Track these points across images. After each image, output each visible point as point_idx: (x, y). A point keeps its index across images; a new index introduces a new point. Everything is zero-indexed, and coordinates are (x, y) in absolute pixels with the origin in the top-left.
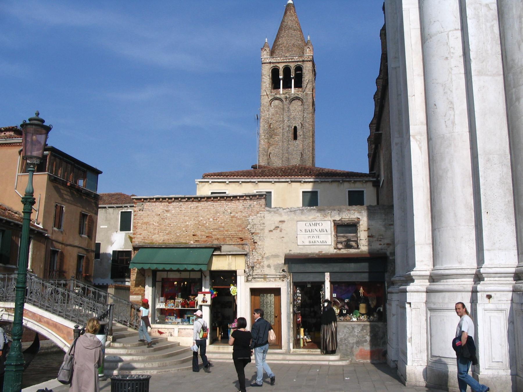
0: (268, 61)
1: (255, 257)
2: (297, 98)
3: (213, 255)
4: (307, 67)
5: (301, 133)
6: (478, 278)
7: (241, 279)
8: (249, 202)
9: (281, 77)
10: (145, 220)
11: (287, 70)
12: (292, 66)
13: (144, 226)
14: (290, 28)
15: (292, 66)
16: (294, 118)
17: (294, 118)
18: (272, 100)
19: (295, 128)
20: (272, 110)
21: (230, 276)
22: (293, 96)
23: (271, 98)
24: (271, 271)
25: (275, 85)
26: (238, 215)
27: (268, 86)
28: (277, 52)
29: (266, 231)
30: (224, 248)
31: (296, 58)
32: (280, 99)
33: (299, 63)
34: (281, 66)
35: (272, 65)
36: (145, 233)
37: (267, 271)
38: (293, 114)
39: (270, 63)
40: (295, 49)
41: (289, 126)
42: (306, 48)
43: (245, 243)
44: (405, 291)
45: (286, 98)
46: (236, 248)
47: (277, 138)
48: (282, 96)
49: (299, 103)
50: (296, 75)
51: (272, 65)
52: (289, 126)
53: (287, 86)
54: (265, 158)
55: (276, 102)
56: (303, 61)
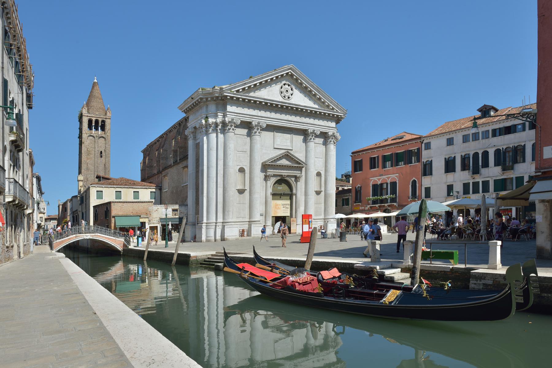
2: (103, 137)
4: (108, 122)
6: (216, 223)
9: (93, 124)
11: (97, 121)
12: (100, 120)
14: (97, 98)
15: (100, 120)
16: (101, 147)
17: (101, 147)
18: (89, 136)
19: (101, 152)
20: (88, 141)
21: (143, 224)
22: (100, 136)
25: (90, 127)
28: (90, 111)
32: (93, 136)
34: (94, 119)
38: (100, 145)
43: (148, 214)
47: (91, 156)
48: (95, 135)
49: (104, 139)
53: (97, 129)
54: (85, 165)
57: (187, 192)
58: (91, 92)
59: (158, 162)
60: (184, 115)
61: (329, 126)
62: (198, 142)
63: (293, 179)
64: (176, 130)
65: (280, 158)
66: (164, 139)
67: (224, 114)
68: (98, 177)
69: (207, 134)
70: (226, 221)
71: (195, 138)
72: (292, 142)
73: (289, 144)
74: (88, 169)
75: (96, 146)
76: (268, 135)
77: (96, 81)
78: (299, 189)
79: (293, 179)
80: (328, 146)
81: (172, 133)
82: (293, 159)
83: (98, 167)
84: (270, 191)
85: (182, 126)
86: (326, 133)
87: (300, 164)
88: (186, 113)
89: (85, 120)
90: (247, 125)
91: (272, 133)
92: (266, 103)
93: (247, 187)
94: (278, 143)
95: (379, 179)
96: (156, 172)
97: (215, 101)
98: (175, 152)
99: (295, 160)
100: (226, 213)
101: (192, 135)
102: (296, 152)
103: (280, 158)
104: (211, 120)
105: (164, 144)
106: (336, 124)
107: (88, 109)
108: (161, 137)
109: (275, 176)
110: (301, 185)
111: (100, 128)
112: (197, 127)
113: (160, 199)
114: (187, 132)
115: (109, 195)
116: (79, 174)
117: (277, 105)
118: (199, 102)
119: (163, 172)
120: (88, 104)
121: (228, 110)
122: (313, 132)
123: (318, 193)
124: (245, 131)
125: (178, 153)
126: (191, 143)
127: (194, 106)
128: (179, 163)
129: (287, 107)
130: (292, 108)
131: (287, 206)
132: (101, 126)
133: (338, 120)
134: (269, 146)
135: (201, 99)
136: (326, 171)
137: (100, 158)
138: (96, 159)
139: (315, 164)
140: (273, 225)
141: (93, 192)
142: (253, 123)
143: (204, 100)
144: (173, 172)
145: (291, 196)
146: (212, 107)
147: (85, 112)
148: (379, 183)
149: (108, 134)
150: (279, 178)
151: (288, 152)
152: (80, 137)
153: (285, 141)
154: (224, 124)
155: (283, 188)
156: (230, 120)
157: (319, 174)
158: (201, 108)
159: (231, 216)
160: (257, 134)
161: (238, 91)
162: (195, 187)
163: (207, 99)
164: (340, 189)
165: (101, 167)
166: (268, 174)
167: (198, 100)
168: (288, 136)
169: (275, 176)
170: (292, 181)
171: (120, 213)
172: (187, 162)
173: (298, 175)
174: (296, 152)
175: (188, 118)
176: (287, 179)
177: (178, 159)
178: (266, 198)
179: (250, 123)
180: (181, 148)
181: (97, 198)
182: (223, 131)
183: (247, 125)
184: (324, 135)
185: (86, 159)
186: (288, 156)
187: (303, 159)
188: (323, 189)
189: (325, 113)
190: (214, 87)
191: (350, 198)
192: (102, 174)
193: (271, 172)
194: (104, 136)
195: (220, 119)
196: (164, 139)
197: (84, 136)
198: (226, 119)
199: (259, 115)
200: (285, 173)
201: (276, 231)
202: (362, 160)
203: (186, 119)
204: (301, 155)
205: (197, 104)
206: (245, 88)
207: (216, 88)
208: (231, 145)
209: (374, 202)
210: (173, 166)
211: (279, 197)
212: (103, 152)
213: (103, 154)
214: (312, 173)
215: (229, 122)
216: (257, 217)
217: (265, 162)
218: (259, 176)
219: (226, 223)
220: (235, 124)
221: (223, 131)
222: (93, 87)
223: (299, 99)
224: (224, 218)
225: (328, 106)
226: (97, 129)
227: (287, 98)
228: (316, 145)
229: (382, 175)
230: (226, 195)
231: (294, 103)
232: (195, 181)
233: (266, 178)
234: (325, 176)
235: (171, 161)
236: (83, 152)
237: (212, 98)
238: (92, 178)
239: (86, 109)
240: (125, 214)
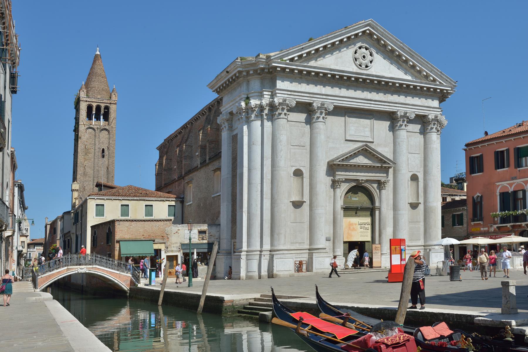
0: (84, 99)
4: (113, 108)
5: (107, 154)
6: (261, 251)
9: (94, 112)
11: (98, 108)
12: (103, 105)
15: (103, 105)
16: (103, 143)
17: (103, 143)
18: (88, 128)
19: (103, 150)
20: (87, 136)
22: (103, 127)
23: (87, 127)
25: (89, 116)
26: (161, 227)
27: (84, 118)
28: (90, 94)
31: (105, 101)
33: (107, 105)
34: (94, 105)
35: (88, 103)
38: (102, 140)
39: (86, 101)
40: (104, 92)
41: (99, 148)
42: (112, 94)
44: (240, 255)
45: (98, 128)
47: (90, 156)
48: (95, 127)
49: (107, 133)
50: (104, 111)
51: (88, 103)
52: (99, 148)
53: (98, 118)
54: (82, 169)
55: (90, 130)
56: (110, 103)
57: (219, 206)
58: (92, 68)
59: (180, 162)
60: (215, 96)
61: (430, 106)
62: (235, 133)
63: (375, 186)
64: (205, 117)
65: (356, 155)
66: (187, 131)
67: (272, 92)
68: (99, 185)
69: (248, 121)
70: (276, 248)
71: (231, 128)
72: (372, 130)
73: (368, 133)
74: (85, 174)
75: (97, 143)
76: (336, 122)
77: (98, 53)
78: (385, 200)
79: (375, 186)
80: (428, 136)
81: (199, 121)
82: (374, 155)
83: (98, 171)
84: (340, 203)
85: (213, 112)
87: (385, 162)
88: (218, 93)
89: (83, 107)
90: (306, 108)
91: (343, 118)
92: (333, 76)
93: (306, 198)
94: (352, 132)
95: (511, 185)
96: (176, 177)
97: (259, 74)
98: (203, 148)
99: (378, 157)
100: (276, 236)
101: (226, 124)
103: (356, 155)
104: (254, 102)
105: (188, 137)
106: (440, 102)
107: (87, 92)
108: (184, 127)
109: (347, 181)
110: (387, 194)
111: (102, 117)
112: (234, 112)
113: (181, 217)
114: (219, 120)
115: (112, 210)
116: (74, 181)
117: (349, 78)
118: (238, 77)
119: (186, 178)
120: (87, 85)
121: (278, 87)
122: (405, 116)
123: (414, 206)
124: (302, 117)
125: (207, 150)
126: (225, 135)
127: (228, 84)
128: (208, 164)
129: (364, 80)
130: (372, 81)
131: (367, 226)
132: (104, 115)
133: (442, 96)
134: (337, 137)
135: (240, 72)
136: (426, 173)
137: (101, 159)
138: (96, 160)
139: (409, 162)
140: (346, 255)
141: (91, 206)
142: (314, 104)
143: (244, 73)
144: (200, 176)
145: (372, 211)
146: (255, 84)
147: (83, 95)
148: (511, 190)
149: (112, 125)
150: (354, 184)
151: (366, 145)
152: (76, 130)
153: (361, 130)
154: (272, 107)
155: (360, 199)
156: (281, 101)
157: (414, 178)
158: (239, 85)
159: (282, 241)
160: (321, 119)
162: (230, 198)
163: (248, 72)
164: (449, 199)
165: (103, 172)
166: (337, 178)
167: (235, 75)
168: (366, 122)
169: (347, 181)
170: (373, 188)
172: (220, 162)
173: (383, 180)
175: (221, 99)
176: (367, 185)
177: (208, 158)
178: (334, 215)
179: (310, 104)
180: (211, 142)
181: (96, 215)
182: (272, 117)
183: (306, 108)
184: (422, 120)
185: (83, 160)
186: (366, 151)
187: (391, 157)
188: (421, 200)
189: (422, 88)
190: (259, 55)
191: (465, 213)
192: (103, 181)
193: (341, 175)
194: (107, 127)
195: (266, 101)
196: (187, 131)
197: (82, 128)
198: (276, 100)
200: (362, 176)
201: (350, 264)
202: (482, 155)
203: (219, 102)
204: (387, 149)
205: (234, 80)
206: (302, 55)
207: (261, 56)
208: (283, 137)
209: (504, 220)
210: (200, 168)
211: (354, 213)
212: (106, 150)
213: (106, 152)
214: (405, 175)
215: (280, 104)
216: (321, 243)
217: (333, 161)
218: (323, 181)
219: (275, 251)
220: (288, 106)
221: (272, 117)
222: (94, 61)
223: (382, 68)
224: (272, 244)
225: (427, 77)
226: (98, 118)
227: (364, 66)
228: (410, 135)
229: (515, 178)
230: (276, 209)
231: (374, 73)
232: (230, 189)
233: (335, 184)
234: (425, 180)
235: (197, 162)
236: (79, 150)
237: (255, 71)
238: (91, 186)
239: (85, 91)
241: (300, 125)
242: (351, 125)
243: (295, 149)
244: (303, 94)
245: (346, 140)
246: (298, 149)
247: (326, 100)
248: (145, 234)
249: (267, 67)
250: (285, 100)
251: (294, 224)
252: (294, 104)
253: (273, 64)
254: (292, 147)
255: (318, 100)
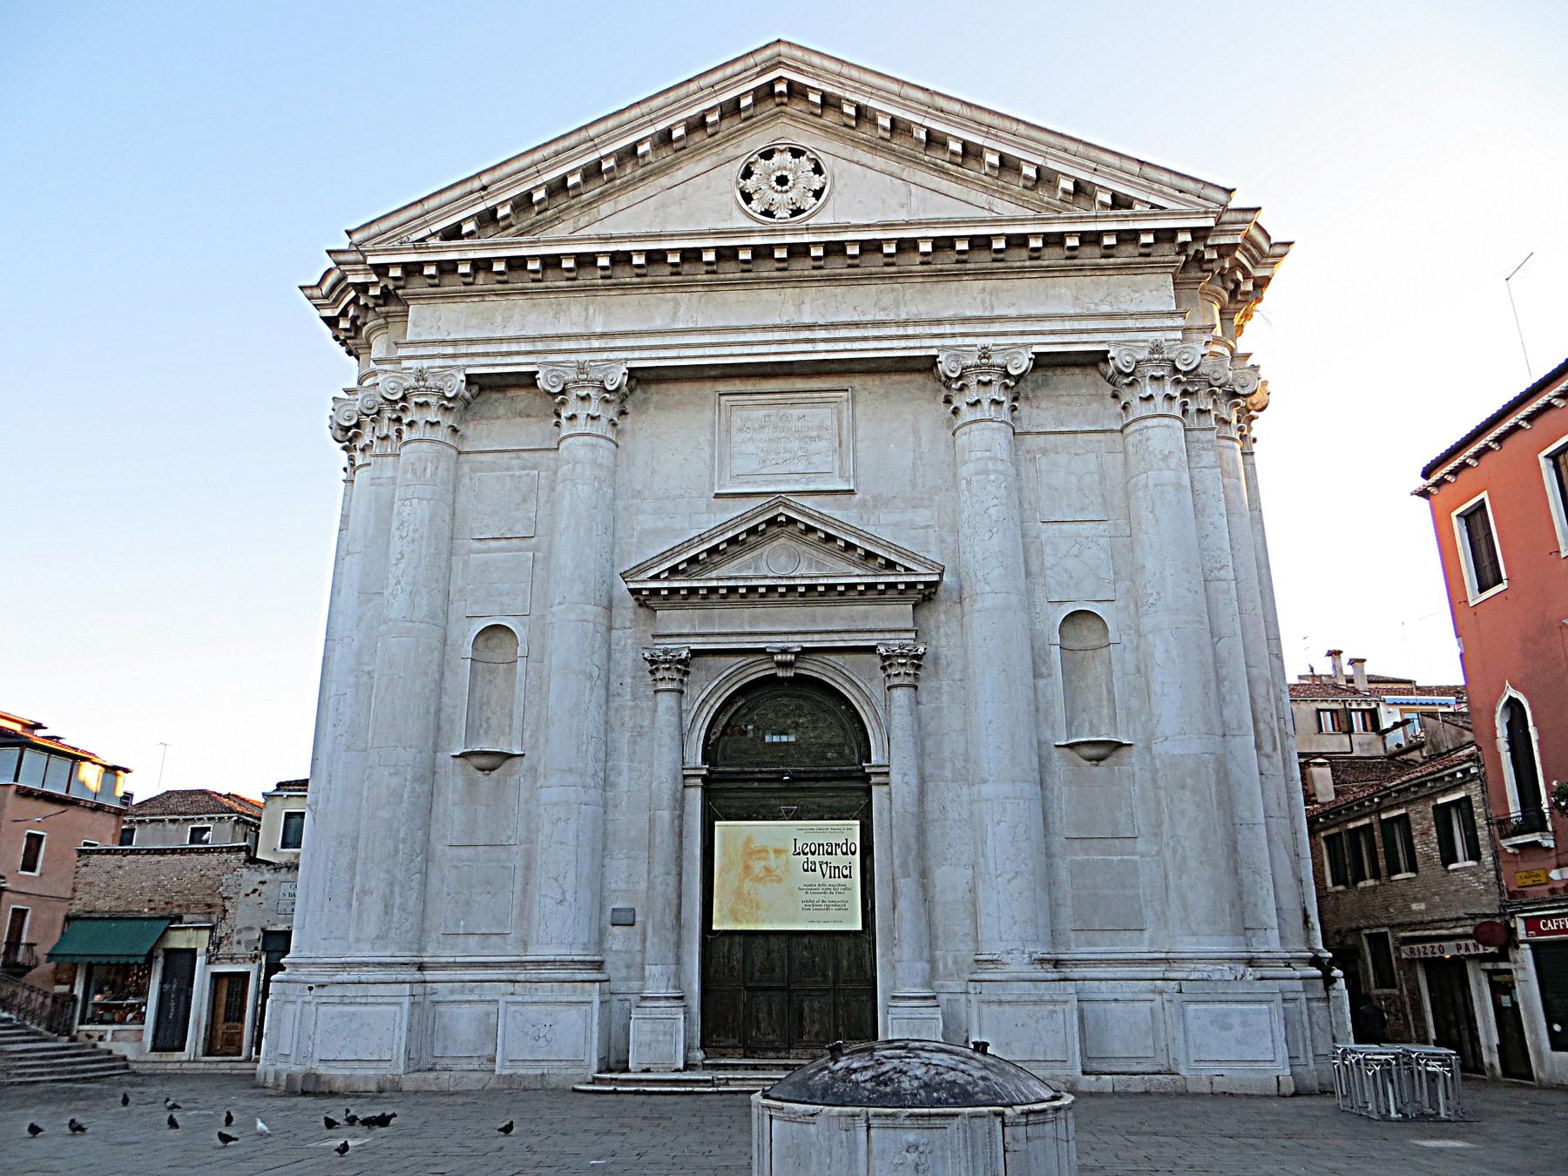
1: (219, 933)
3: (168, 929)
7: (200, 960)
8: (225, 856)
10: (89, 879)
13: (87, 889)
24: (240, 950)
29: (242, 894)
30: (186, 918)
36: (86, 898)
37: (235, 949)
43: (214, 911)
46: (201, 918)
86: (1103, 356)
87: (890, 565)
102: (879, 502)
153: (780, 449)
161: (453, 233)
171: (104, 905)
174: (879, 502)
176: (810, 668)
199: (599, 330)
204: (922, 516)
240: (119, 906)
241: (515, 462)
242: (746, 436)
243: (488, 551)
244: (505, 348)
245: (717, 496)
246: (501, 550)
247: (605, 356)
248: (156, 898)
249: (374, 278)
250: (421, 375)
251: (463, 852)
252: (456, 385)
253: (371, 260)
254: (477, 545)
255: (573, 357)
